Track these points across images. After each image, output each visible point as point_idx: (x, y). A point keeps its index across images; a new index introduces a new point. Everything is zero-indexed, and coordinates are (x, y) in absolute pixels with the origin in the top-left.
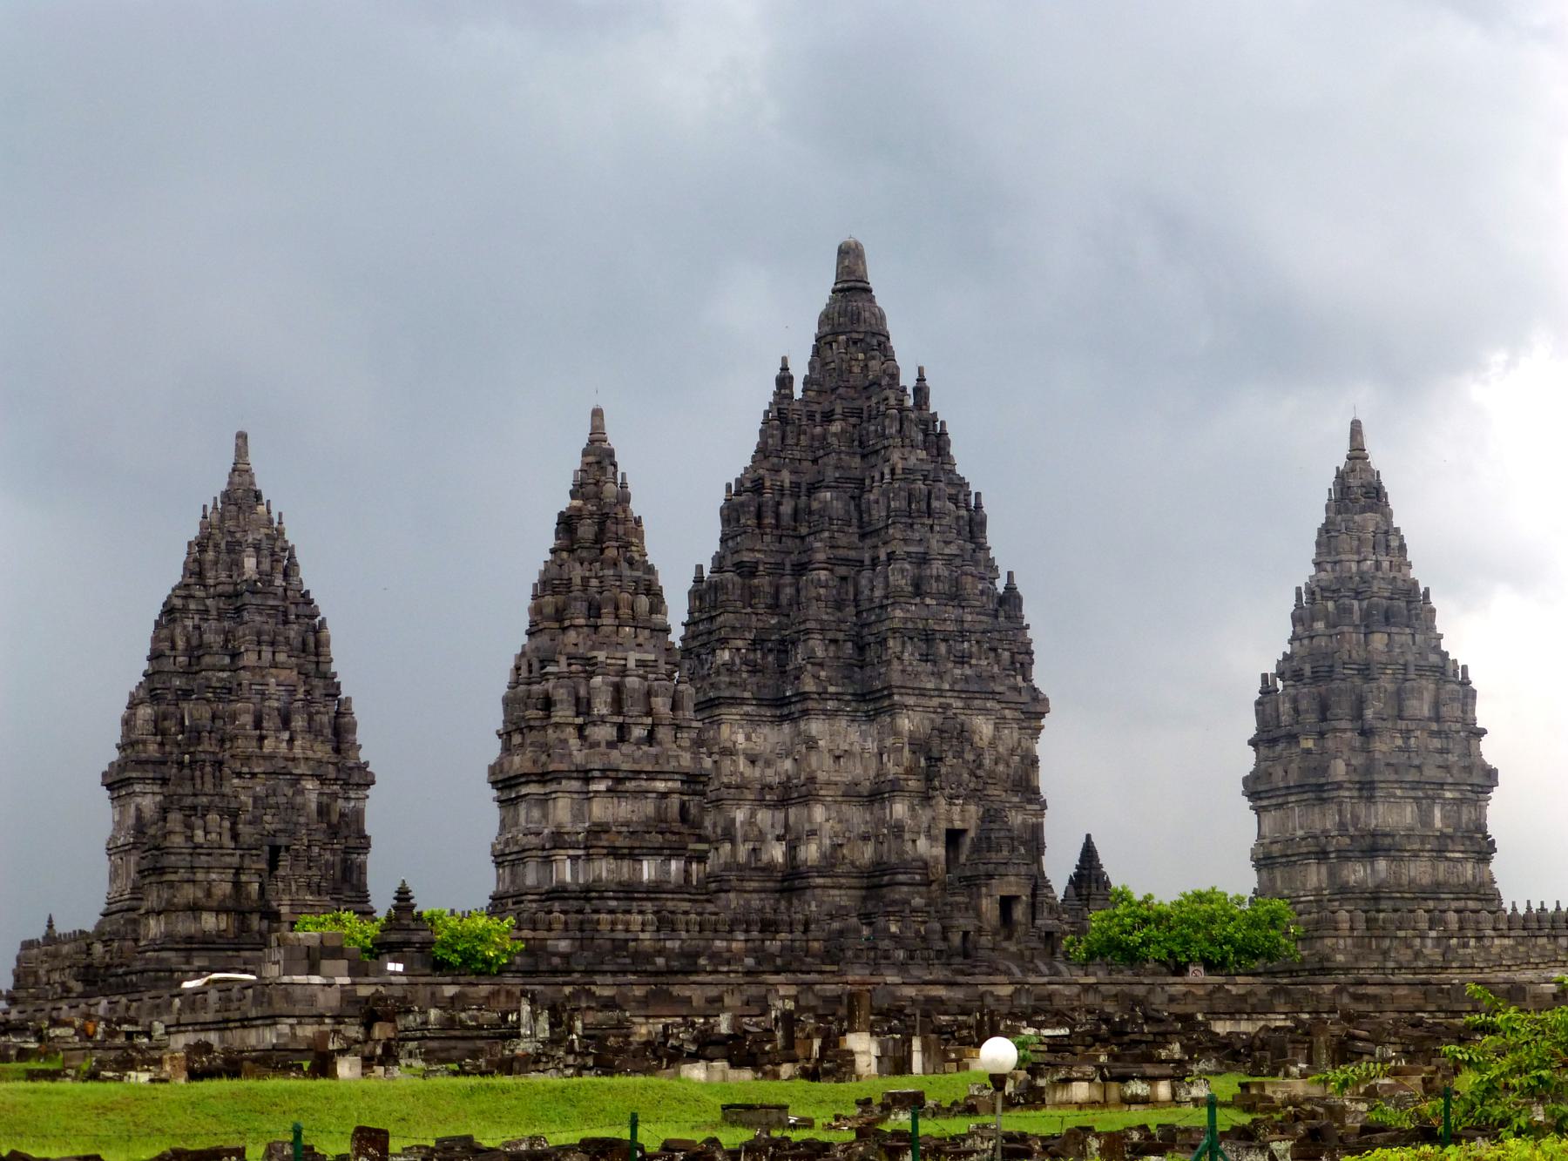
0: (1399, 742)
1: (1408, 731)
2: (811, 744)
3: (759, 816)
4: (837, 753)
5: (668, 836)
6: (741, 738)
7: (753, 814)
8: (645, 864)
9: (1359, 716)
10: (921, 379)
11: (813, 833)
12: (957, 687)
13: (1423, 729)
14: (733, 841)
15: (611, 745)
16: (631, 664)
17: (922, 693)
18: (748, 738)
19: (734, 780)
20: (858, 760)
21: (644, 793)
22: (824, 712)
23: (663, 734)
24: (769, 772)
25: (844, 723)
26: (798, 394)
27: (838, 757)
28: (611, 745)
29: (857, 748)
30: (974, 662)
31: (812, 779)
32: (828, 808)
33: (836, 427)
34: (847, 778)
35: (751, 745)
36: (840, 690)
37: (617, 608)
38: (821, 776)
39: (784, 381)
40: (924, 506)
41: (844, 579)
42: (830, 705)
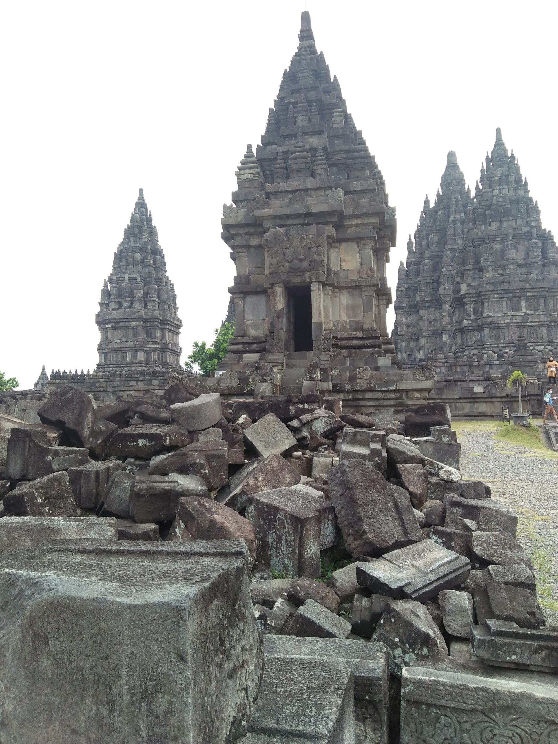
0: (500, 272)
1: (504, 266)
3: (411, 344)
5: (135, 342)
6: (404, 319)
7: (409, 343)
8: (127, 353)
9: (478, 262)
11: (422, 347)
13: (513, 264)
14: (401, 352)
15: (114, 310)
16: (127, 279)
18: (407, 319)
19: (403, 333)
21: (127, 327)
22: (425, 307)
23: (136, 305)
24: (415, 329)
25: (433, 310)
26: (432, 204)
27: (431, 322)
28: (114, 310)
31: (421, 330)
32: (427, 339)
35: (408, 321)
36: (430, 299)
37: (127, 259)
38: (424, 329)
39: (427, 202)
40: (460, 231)
41: (438, 262)
42: (427, 304)
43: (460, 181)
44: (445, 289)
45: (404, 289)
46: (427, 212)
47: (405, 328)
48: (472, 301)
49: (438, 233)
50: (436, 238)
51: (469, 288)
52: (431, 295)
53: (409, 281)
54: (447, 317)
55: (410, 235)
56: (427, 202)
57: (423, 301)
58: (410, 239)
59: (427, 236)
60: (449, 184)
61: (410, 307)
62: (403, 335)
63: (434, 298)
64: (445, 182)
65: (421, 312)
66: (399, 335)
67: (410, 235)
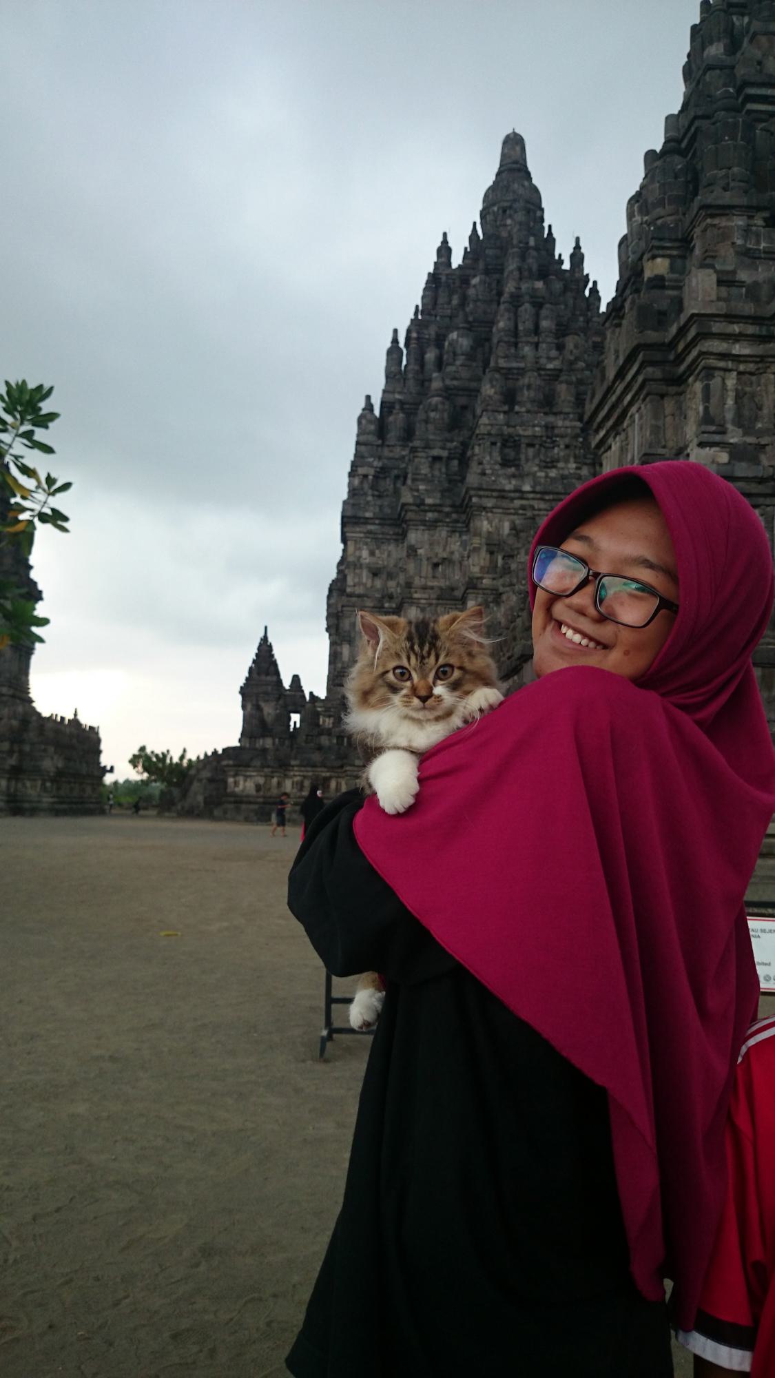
2: (412, 551)
4: (435, 560)
10: (577, 247)
12: (538, 489)
17: (502, 495)
18: (372, 554)
20: (457, 567)
22: (424, 522)
24: (392, 584)
25: (444, 534)
26: (457, 260)
27: (436, 565)
29: (456, 556)
30: (561, 465)
31: (409, 585)
33: (475, 281)
34: (442, 583)
35: (374, 560)
36: (438, 501)
38: (417, 582)
39: (444, 250)
40: (529, 325)
41: (464, 408)
42: (430, 515)
43: (533, 205)
44: (483, 474)
45: (371, 471)
46: (444, 278)
47: (365, 576)
48: (737, 358)
49: (469, 329)
50: (465, 343)
51: (724, 291)
52: (443, 492)
53: (386, 452)
54: (484, 553)
55: (396, 331)
56: (444, 250)
57: (420, 504)
58: (395, 341)
59: (439, 341)
60: (504, 211)
61: (383, 520)
62: (359, 596)
63: (448, 502)
64: (494, 205)
65: (413, 537)
66: (350, 595)
67: (396, 331)
